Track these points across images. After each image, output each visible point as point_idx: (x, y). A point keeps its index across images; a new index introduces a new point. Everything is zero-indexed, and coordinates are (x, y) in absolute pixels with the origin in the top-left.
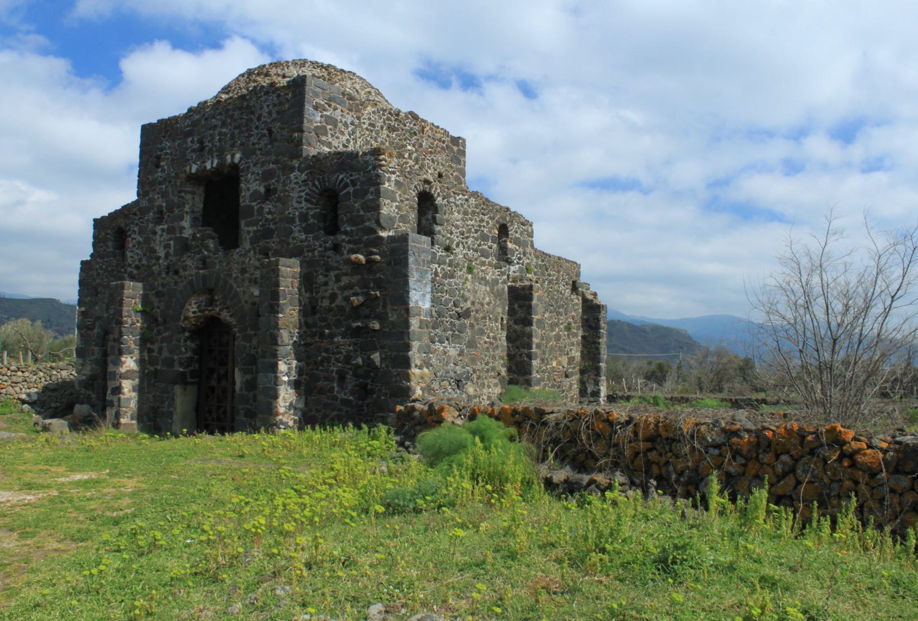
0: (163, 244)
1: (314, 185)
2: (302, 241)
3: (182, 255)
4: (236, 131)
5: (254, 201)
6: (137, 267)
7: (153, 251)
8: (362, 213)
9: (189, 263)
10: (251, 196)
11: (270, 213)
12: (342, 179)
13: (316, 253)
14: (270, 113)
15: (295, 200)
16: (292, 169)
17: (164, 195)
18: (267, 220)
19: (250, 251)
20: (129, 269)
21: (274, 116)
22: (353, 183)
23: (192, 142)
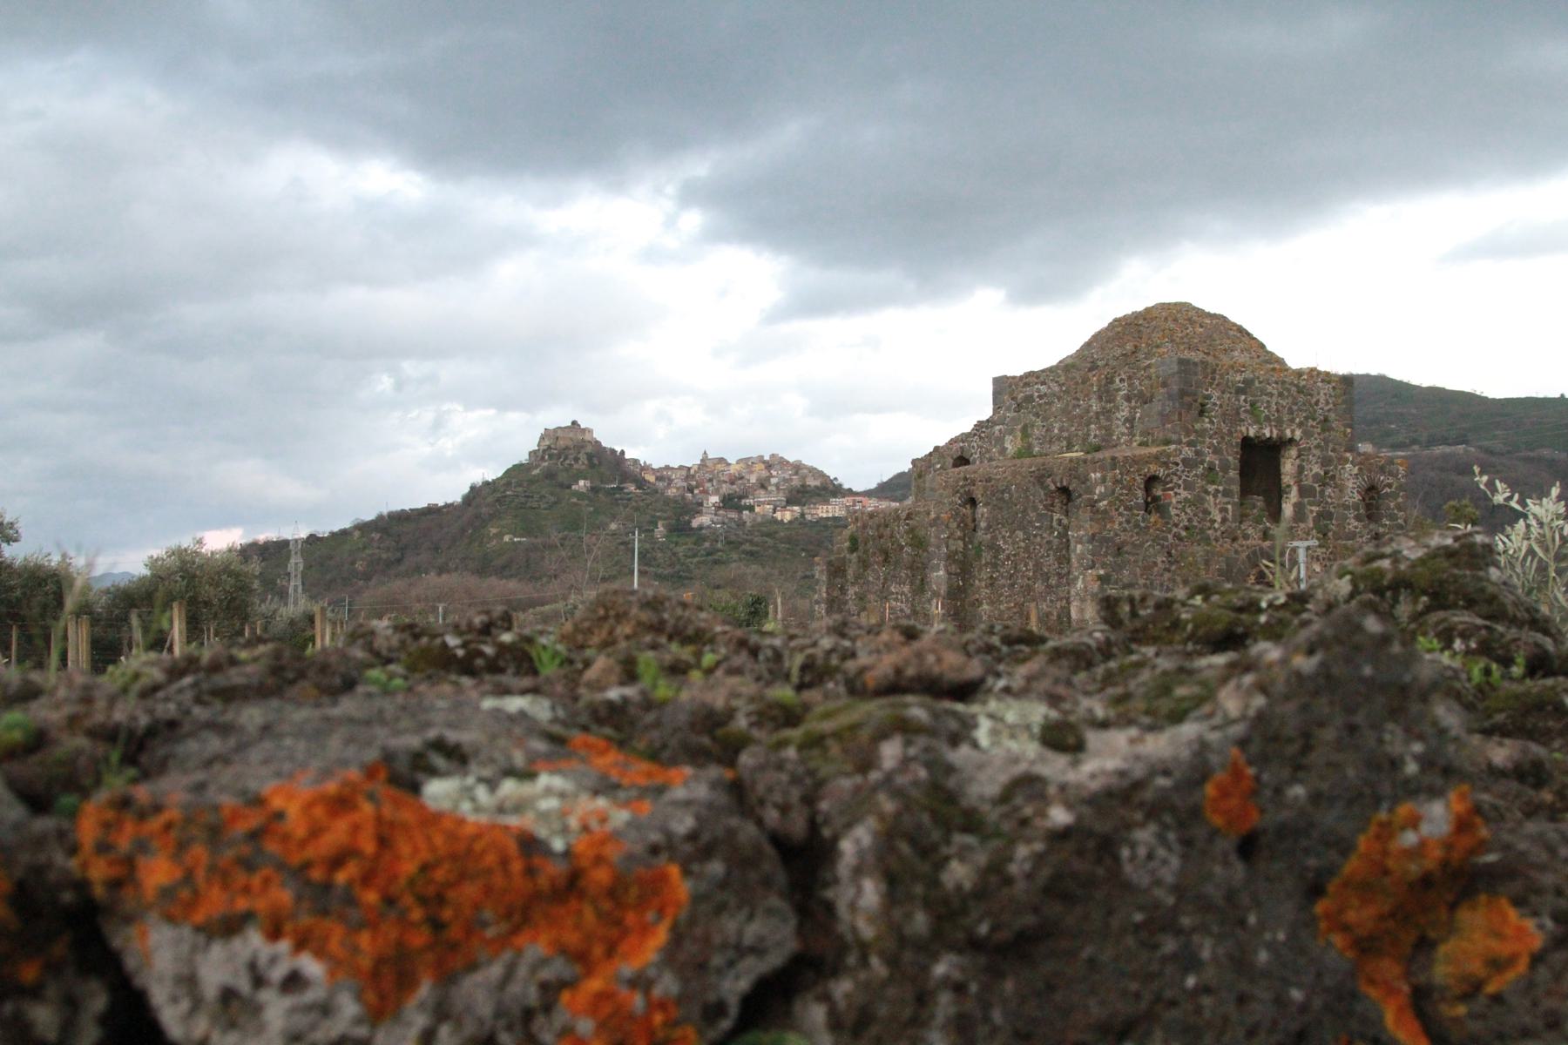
0: (1218, 506)
1: (1364, 480)
2: (1356, 527)
3: (1241, 523)
4: (1295, 408)
5: (1317, 483)
6: (1187, 528)
7: (1206, 512)
8: (1396, 511)
9: (1250, 531)
10: (1313, 476)
11: (1330, 497)
12: (1383, 481)
13: (1364, 538)
14: (1327, 403)
15: (1349, 490)
16: (1346, 461)
17: (1216, 451)
18: (1327, 503)
19: (1312, 529)
20: (1175, 530)
21: (1331, 406)
22: (1390, 486)
23: (1245, 401)
